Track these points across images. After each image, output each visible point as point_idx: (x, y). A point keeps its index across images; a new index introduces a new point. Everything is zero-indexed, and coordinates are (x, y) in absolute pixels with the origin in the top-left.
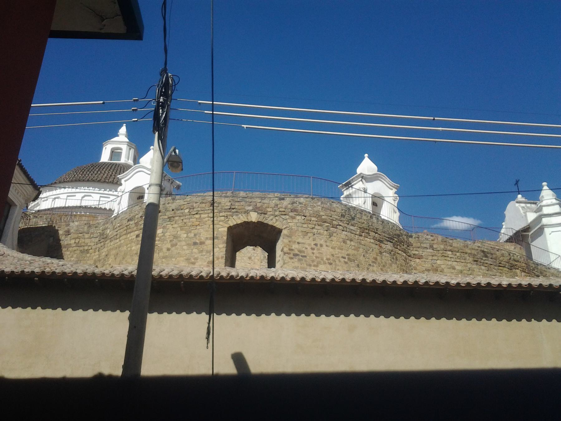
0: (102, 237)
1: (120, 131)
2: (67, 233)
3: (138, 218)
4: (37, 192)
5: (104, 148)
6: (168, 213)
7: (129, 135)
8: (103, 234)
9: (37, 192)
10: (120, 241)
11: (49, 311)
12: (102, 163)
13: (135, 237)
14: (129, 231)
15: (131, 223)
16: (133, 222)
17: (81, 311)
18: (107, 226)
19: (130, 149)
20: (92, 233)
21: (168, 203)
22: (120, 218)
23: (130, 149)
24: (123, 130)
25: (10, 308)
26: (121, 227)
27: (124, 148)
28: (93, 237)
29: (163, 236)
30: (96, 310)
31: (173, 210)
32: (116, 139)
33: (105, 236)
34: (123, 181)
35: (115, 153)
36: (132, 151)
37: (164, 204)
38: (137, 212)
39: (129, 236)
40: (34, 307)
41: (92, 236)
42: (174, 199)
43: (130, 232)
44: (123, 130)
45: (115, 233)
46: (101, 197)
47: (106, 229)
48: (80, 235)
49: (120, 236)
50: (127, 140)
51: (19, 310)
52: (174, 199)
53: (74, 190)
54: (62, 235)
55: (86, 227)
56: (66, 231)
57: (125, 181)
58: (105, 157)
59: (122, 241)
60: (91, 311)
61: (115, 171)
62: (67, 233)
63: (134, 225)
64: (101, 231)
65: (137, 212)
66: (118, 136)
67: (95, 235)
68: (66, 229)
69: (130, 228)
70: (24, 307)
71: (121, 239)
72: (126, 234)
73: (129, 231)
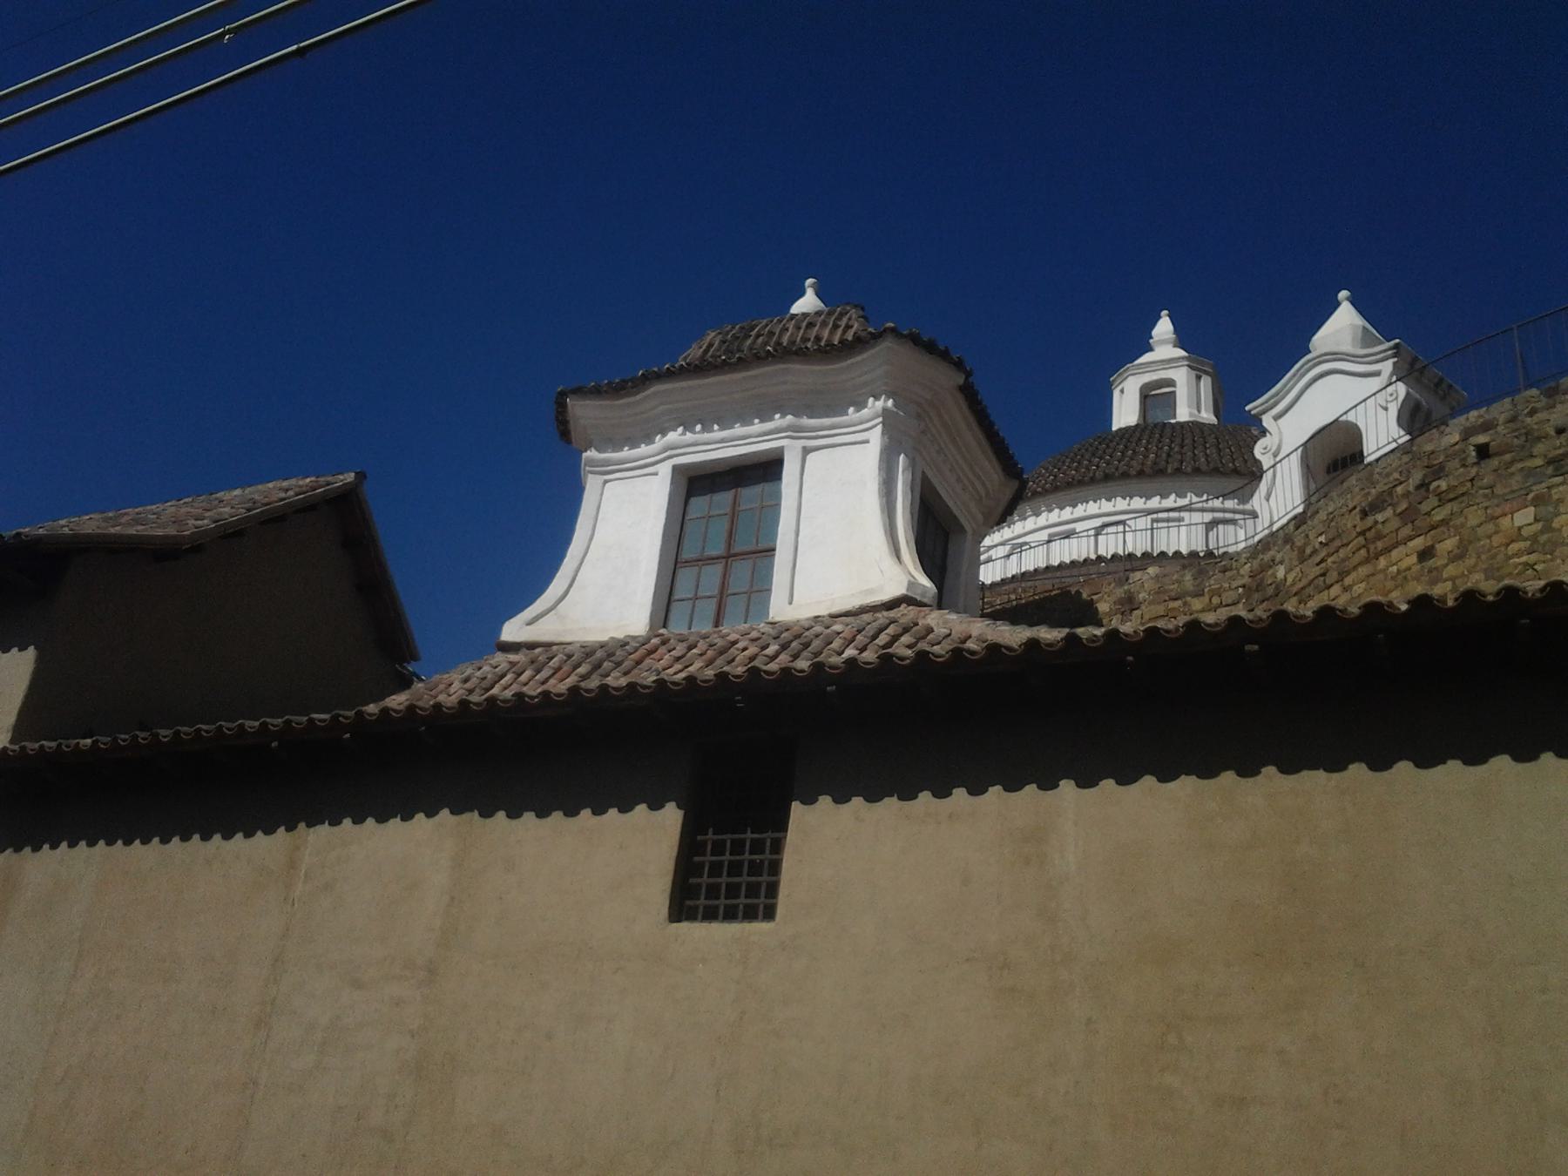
0: (1256, 596)
1: (1154, 333)
2: (1127, 607)
3: (1407, 495)
4: (1015, 484)
5: (1116, 393)
6: (1539, 448)
7: (1182, 340)
8: (1259, 587)
9: (1015, 484)
10: (1346, 589)
11: (1314, 781)
12: (1120, 430)
13: (1414, 559)
14: (1380, 545)
15: (1380, 517)
16: (1389, 512)
17: (1454, 765)
18: (1267, 557)
19: (1199, 378)
20: (1213, 593)
21: (1532, 413)
22: (1322, 515)
23: (1199, 378)
24: (1164, 327)
25: (1149, 781)
26: (1337, 543)
27: (1181, 377)
28: (1221, 605)
29: (1542, 532)
30: (1525, 753)
31: (1560, 431)
32: (1146, 358)
33: (1270, 590)
34: (1267, 421)
35: (1156, 398)
36: (1206, 383)
37: (1513, 419)
38: (1396, 475)
39: (1382, 562)
40: (1248, 770)
41: (1216, 600)
42: (1552, 393)
43: (1388, 550)
44: (1164, 327)
45: (1317, 570)
46: (1153, 521)
47: (1273, 563)
48: (1173, 605)
49: (1343, 574)
50: (1181, 353)
51: (1186, 785)
52: (1552, 393)
53: (1067, 514)
54: (1110, 614)
55: (1188, 577)
56: (1120, 602)
57: (1277, 418)
58: (1125, 412)
59: (1359, 589)
60: (1502, 764)
61: (1178, 440)
62: (1127, 607)
63: (1395, 523)
64: (1246, 580)
65: (1396, 475)
66: (1151, 349)
67: (1229, 597)
68: (1120, 592)
69: (1379, 537)
70: (1207, 771)
71: (1348, 581)
72: (1367, 561)
73: (1380, 545)
